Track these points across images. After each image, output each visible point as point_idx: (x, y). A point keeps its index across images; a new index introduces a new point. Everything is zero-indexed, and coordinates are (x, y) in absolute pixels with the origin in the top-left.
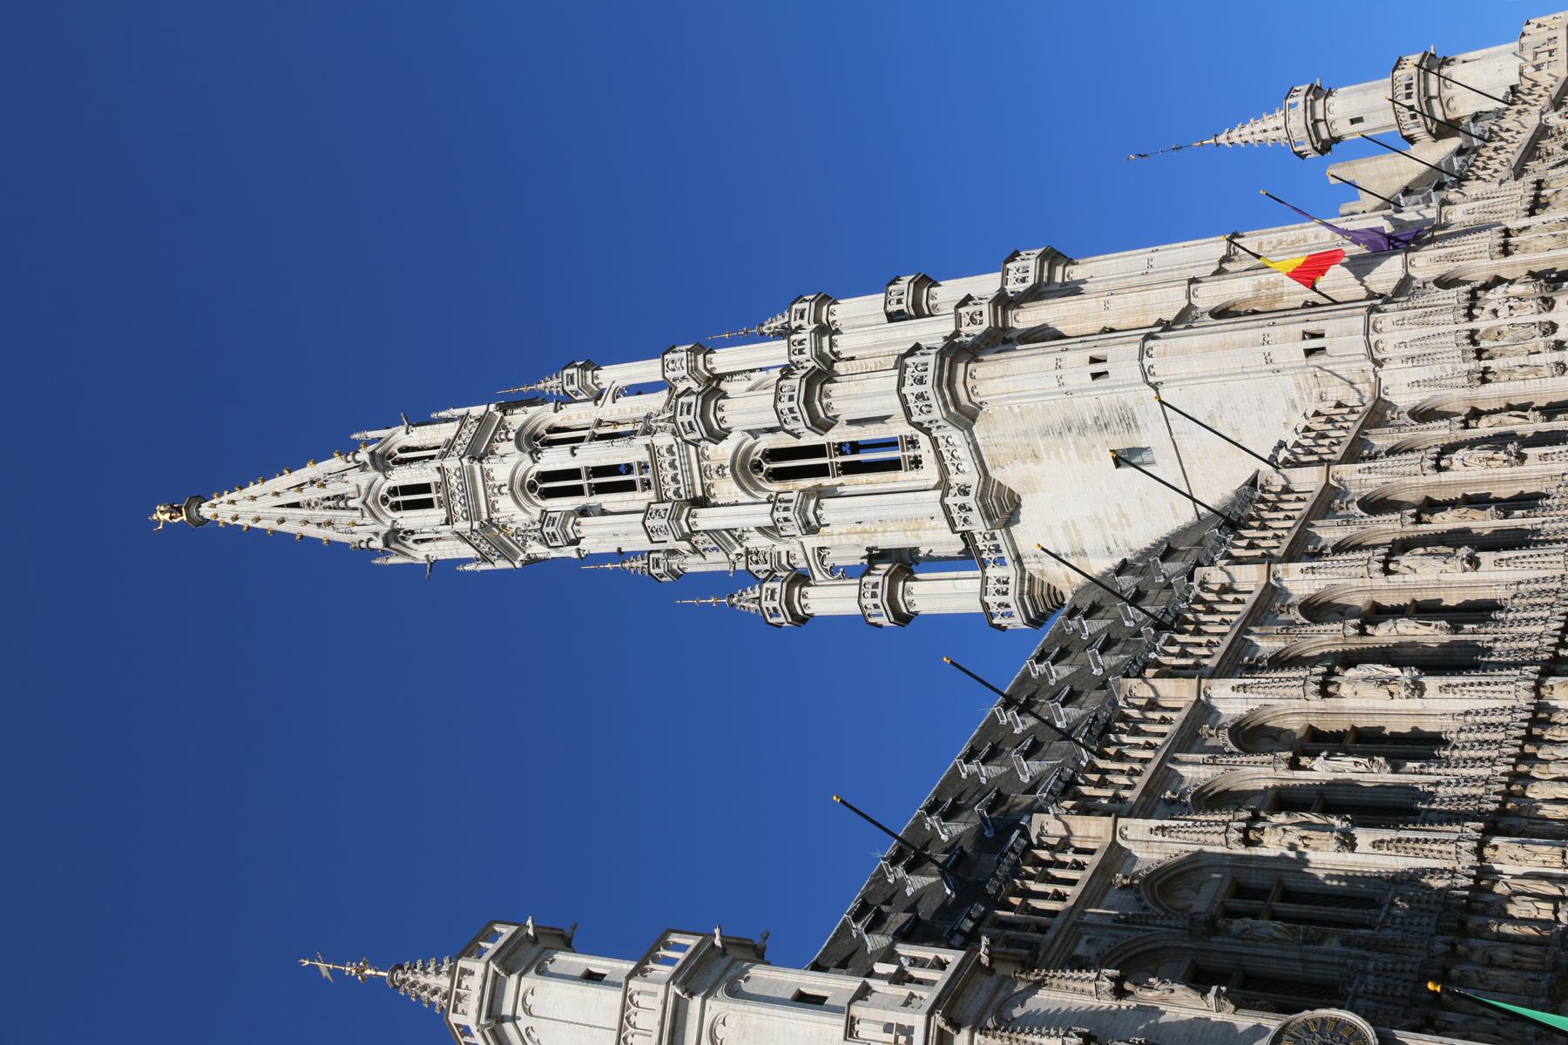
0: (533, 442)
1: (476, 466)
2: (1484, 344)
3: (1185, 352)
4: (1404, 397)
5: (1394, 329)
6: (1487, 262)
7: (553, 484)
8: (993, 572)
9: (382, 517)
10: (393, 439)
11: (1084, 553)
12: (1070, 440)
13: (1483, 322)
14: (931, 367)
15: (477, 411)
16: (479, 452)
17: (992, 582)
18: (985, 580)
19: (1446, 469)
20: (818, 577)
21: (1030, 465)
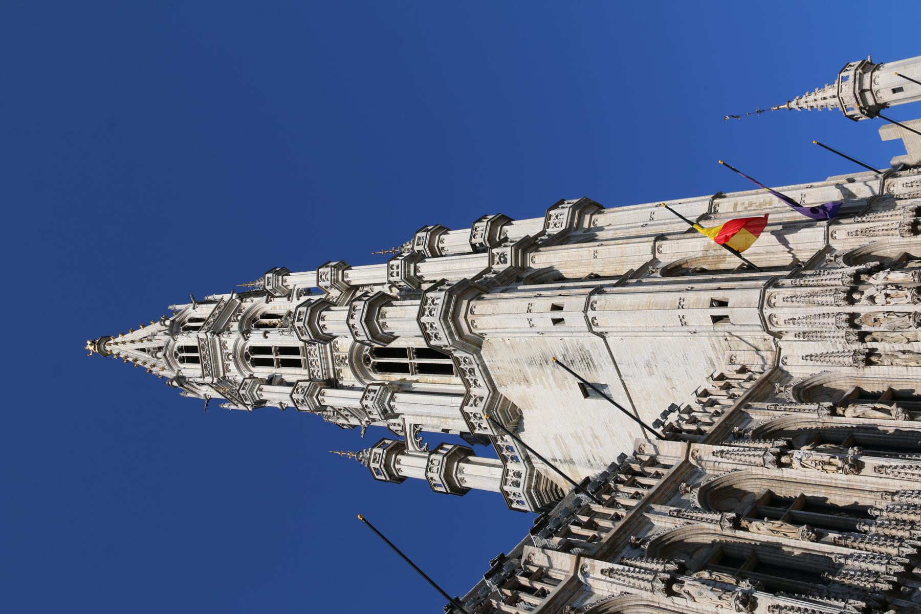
0: (251, 323)
1: (217, 339)
2: (865, 328)
3: (619, 309)
4: (800, 371)
5: (787, 306)
6: (898, 240)
7: (258, 356)
8: (511, 466)
9: (174, 367)
10: (187, 312)
11: (572, 462)
12: (549, 372)
13: (862, 308)
14: (439, 302)
15: (227, 297)
16: (218, 327)
17: (511, 473)
18: (506, 472)
19: (788, 465)
20: (411, 448)
21: (524, 387)
